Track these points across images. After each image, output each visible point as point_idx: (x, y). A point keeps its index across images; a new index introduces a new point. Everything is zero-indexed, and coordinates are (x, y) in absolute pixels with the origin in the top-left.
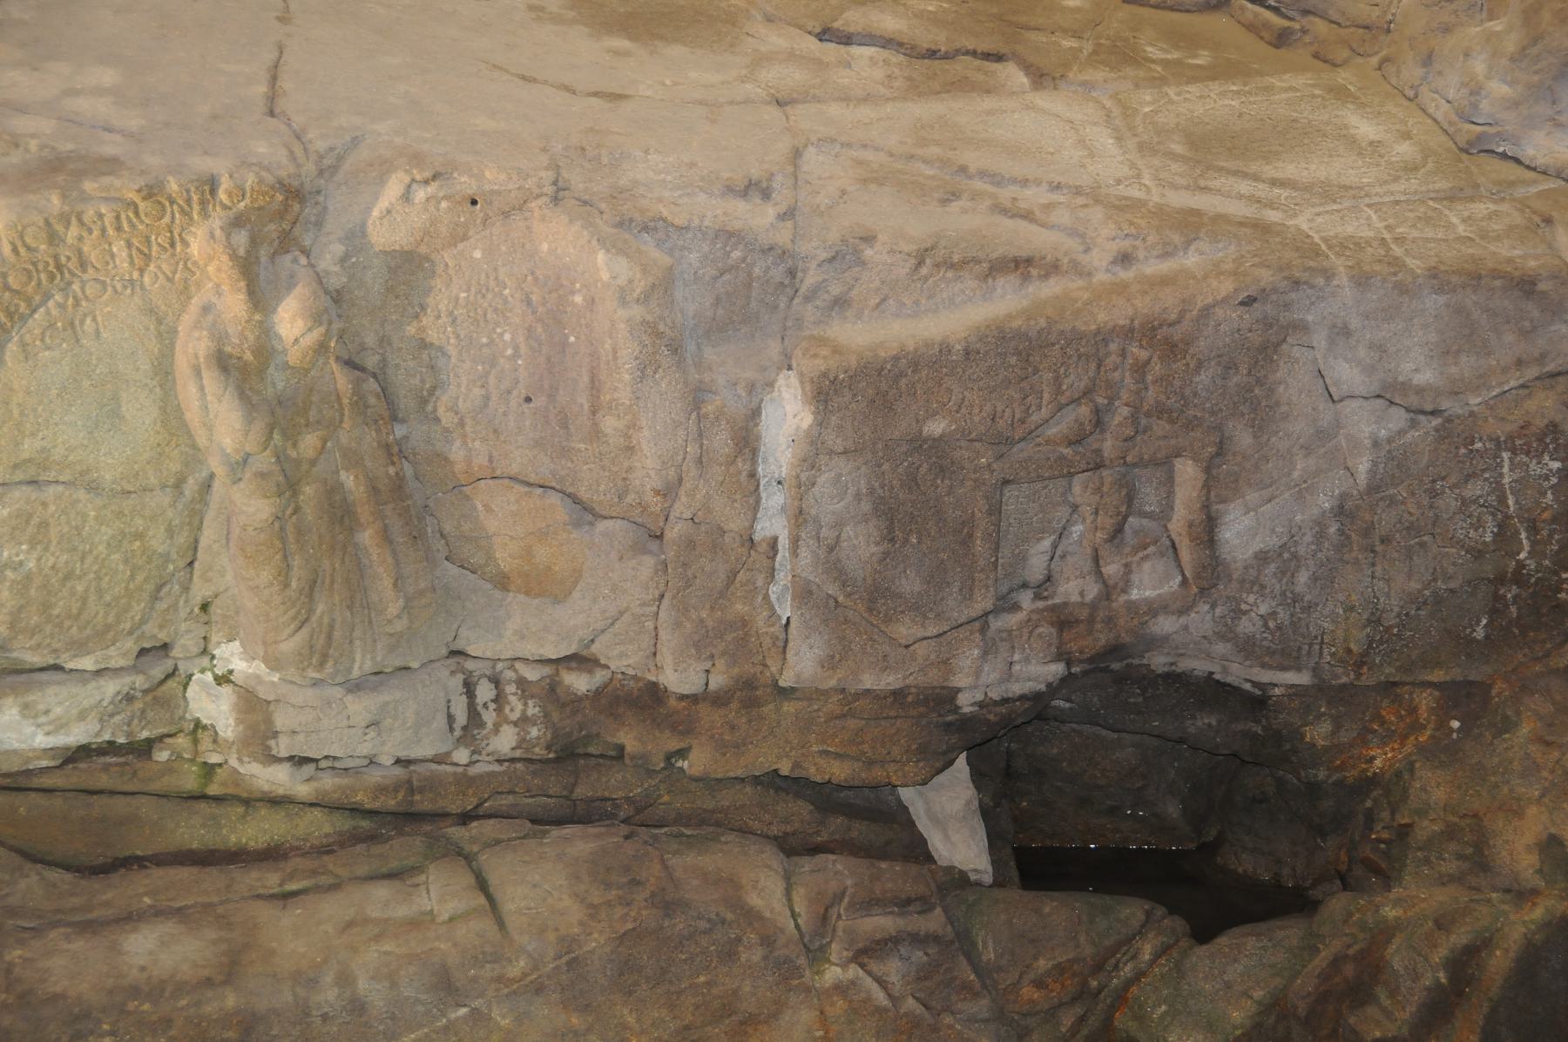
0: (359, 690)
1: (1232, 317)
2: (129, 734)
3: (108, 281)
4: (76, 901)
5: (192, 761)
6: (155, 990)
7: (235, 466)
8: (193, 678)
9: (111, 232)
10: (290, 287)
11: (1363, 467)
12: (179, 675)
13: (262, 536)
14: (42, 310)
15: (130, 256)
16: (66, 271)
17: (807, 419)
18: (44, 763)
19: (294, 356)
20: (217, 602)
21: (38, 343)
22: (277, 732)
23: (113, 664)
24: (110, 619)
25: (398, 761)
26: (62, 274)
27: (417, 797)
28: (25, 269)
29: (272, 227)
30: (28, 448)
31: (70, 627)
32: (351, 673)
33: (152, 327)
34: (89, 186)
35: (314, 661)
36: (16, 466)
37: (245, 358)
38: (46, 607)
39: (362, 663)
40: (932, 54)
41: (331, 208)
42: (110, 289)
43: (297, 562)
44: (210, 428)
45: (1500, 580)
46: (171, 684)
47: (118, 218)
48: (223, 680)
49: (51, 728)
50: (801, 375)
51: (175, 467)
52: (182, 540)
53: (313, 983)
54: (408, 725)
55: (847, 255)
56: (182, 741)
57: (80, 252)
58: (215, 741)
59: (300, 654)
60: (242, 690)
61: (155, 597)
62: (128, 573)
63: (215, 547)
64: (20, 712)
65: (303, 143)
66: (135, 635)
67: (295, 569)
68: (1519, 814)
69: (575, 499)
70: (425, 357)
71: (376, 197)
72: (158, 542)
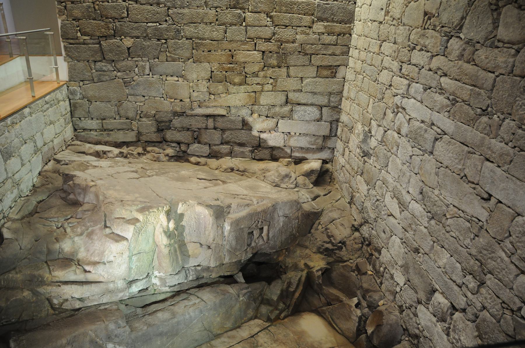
1: (271, 208)
4: (145, 312)
6: (165, 321)
11: (281, 224)
17: (229, 228)
19: (171, 230)
30: (140, 247)
34: (151, 210)
40: (210, 180)
44: (162, 241)
45: (292, 235)
48: (156, 277)
50: (228, 223)
53: (185, 315)
55: (229, 206)
68: (300, 261)
69: (200, 243)
72: (150, 259)
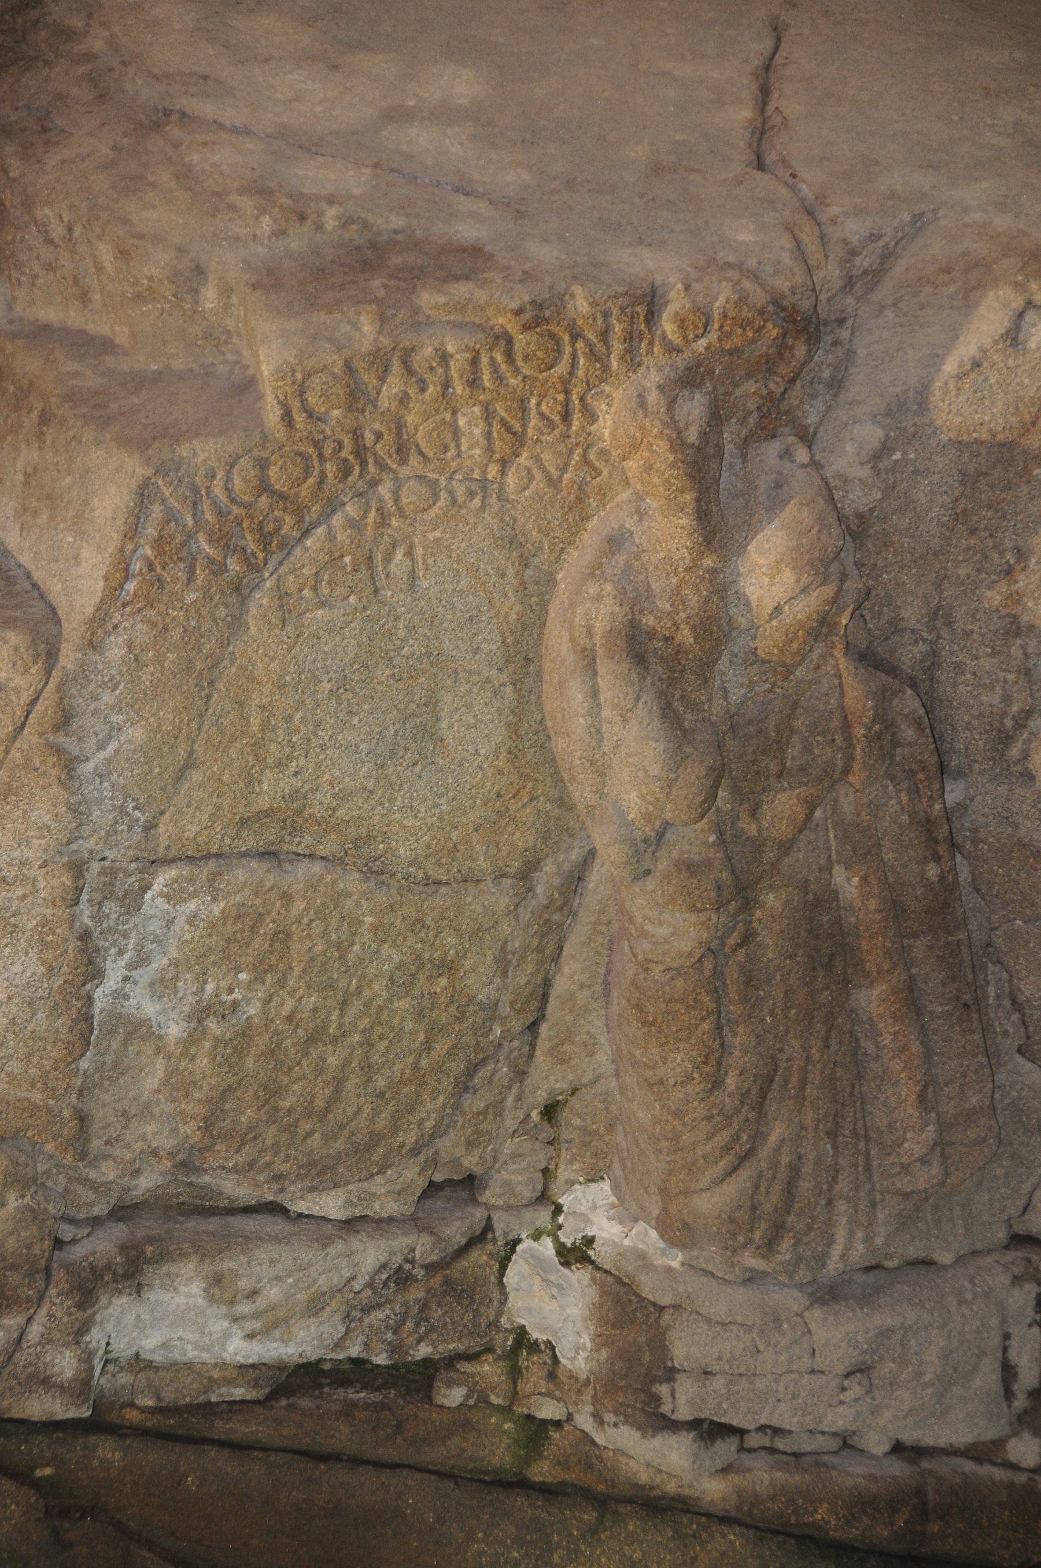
0: (835, 1299)
2: (395, 1349)
3: (443, 481)
5: (506, 1411)
7: (642, 846)
8: (519, 1248)
9: (459, 388)
10: (774, 506)
12: (494, 1240)
13: (679, 984)
14: (321, 531)
15: (488, 435)
16: (371, 460)
18: (238, 1393)
20: (575, 1102)
21: (307, 593)
22: (673, 1370)
23: (379, 1209)
24: (382, 1123)
25: (898, 1448)
26: (363, 464)
27: (935, 1527)
28: (299, 454)
29: (751, 386)
31: (309, 1134)
32: (824, 1265)
33: (511, 572)
34: (428, 299)
35: (757, 1235)
36: (244, 822)
37: (679, 639)
38: (272, 1091)
39: (848, 1247)
41: (862, 352)
42: (443, 495)
43: (740, 1038)
46: (478, 1256)
47: (475, 362)
49: (257, 1325)
51: (523, 839)
52: (523, 981)
54: (927, 1378)
56: (489, 1369)
57: (399, 426)
58: (552, 1376)
59: (732, 1220)
60: (610, 1279)
61: (463, 1086)
62: (421, 1037)
63: (582, 996)
64: (205, 1290)
65: (819, 225)
66: (422, 1158)
67: (737, 1053)
70: (1015, 651)
71: (954, 336)
